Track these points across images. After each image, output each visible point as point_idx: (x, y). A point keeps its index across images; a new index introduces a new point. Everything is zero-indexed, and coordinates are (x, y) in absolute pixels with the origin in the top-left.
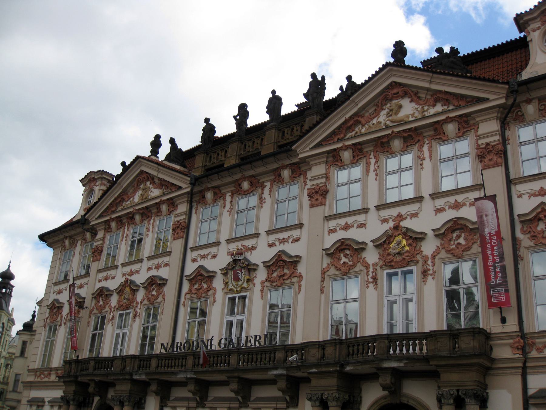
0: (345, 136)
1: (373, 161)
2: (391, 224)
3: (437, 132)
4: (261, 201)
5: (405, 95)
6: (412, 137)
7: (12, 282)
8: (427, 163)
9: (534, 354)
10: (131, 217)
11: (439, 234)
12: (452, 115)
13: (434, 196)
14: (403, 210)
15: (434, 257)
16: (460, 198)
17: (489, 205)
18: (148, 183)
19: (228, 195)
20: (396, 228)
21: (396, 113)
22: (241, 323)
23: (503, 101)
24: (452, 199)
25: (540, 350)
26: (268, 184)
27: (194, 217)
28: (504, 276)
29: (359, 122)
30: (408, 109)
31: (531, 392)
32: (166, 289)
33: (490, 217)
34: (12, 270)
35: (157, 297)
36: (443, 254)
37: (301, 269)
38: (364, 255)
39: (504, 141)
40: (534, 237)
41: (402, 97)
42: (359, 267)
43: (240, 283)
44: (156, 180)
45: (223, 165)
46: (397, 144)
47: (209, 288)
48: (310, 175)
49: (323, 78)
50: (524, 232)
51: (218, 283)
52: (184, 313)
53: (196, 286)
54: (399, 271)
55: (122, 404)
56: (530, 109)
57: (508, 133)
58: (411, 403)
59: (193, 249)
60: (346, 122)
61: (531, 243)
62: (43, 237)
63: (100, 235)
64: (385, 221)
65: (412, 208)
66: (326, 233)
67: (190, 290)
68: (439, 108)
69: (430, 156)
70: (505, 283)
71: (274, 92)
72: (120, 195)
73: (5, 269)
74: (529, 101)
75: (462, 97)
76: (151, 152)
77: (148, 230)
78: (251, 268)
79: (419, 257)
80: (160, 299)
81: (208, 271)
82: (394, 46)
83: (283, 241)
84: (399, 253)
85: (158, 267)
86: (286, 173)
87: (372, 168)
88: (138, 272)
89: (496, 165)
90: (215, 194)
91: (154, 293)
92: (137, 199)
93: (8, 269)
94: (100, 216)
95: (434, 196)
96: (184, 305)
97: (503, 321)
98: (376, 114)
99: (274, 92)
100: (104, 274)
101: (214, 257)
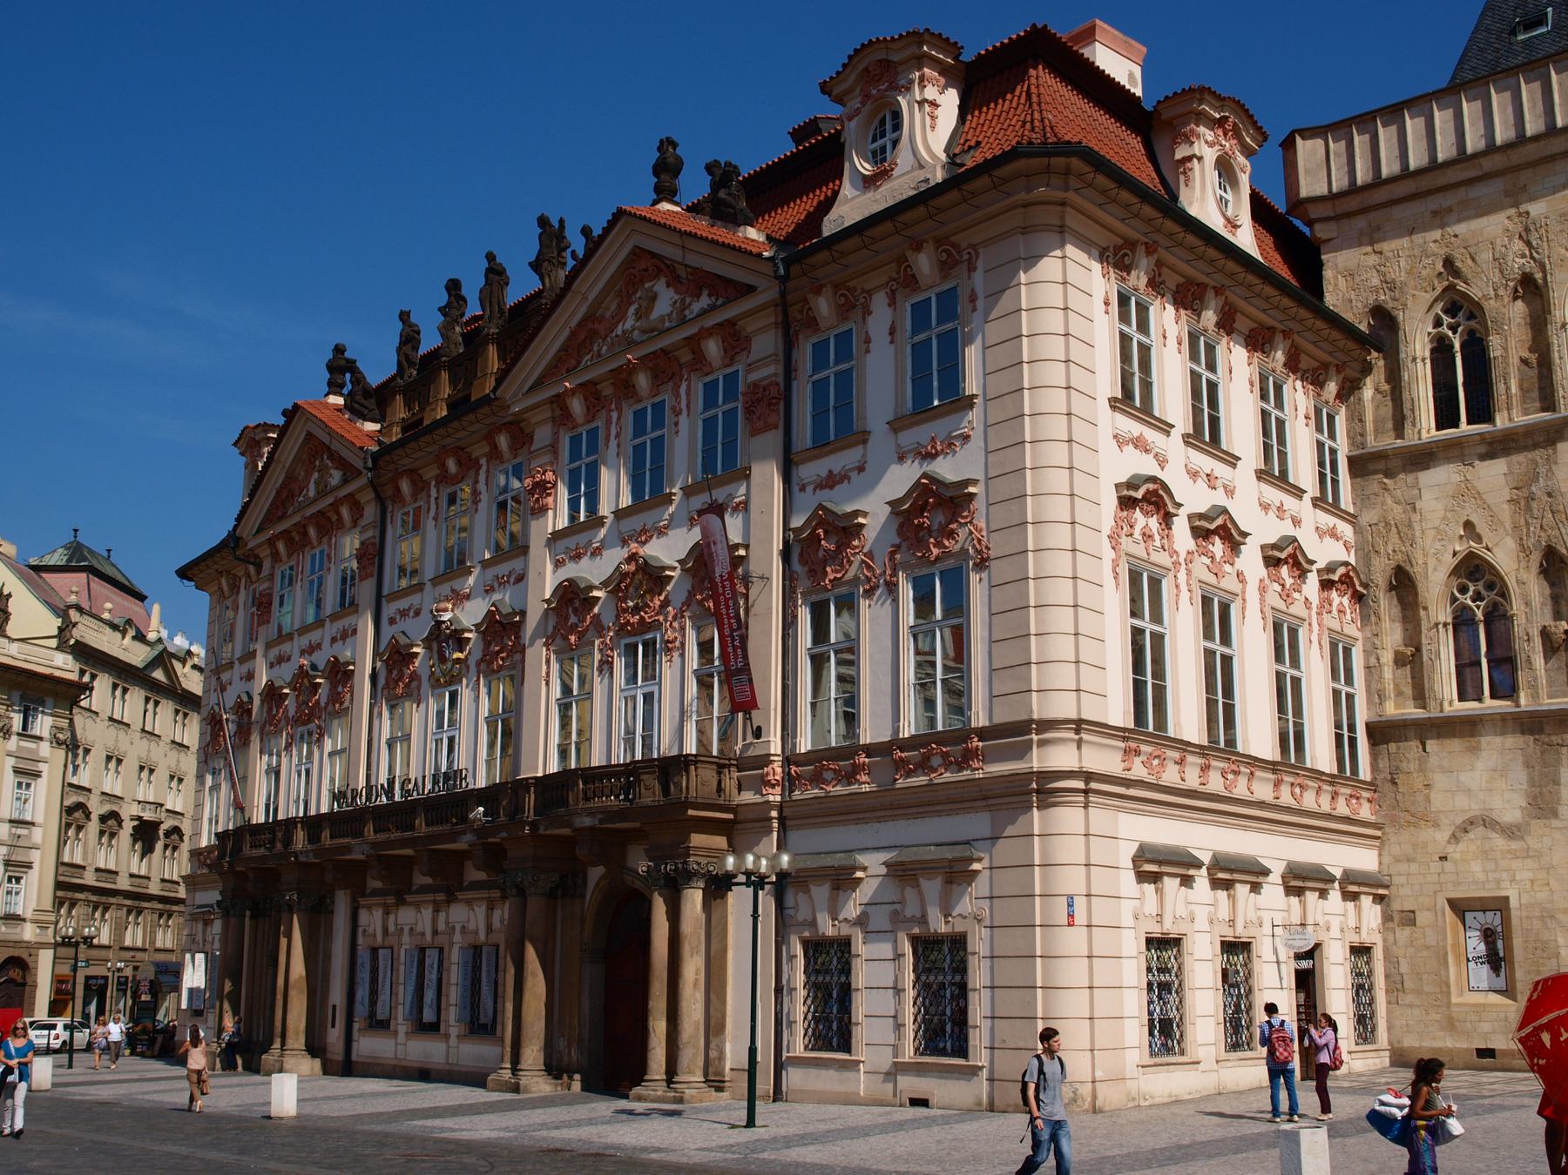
0: (579, 362)
1: (615, 415)
4: (475, 493)
12: (709, 322)
20: (632, 558)
21: (649, 309)
26: (483, 461)
30: (665, 300)
33: (719, 545)
39: (789, 371)
41: (656, 277)
43: (449, 665)
45: (421, 421)
49: (561, 221)
54: (639, 639)
56: (823, 306)
61: (809, 583)
62: (184, 573)
67: (387, 682)
68: (705, 301)
69: (688, 406)
71: (490, 257)
74: (818, 291)
75: (729, 282)
76: (330, 384)
82: (659, 149)
87: (613, 432)
90: (413, 483)
92: (312, 493)
94: (260, 530)
97: (758, 733)
98: (620, 316)
99: (490, 257)
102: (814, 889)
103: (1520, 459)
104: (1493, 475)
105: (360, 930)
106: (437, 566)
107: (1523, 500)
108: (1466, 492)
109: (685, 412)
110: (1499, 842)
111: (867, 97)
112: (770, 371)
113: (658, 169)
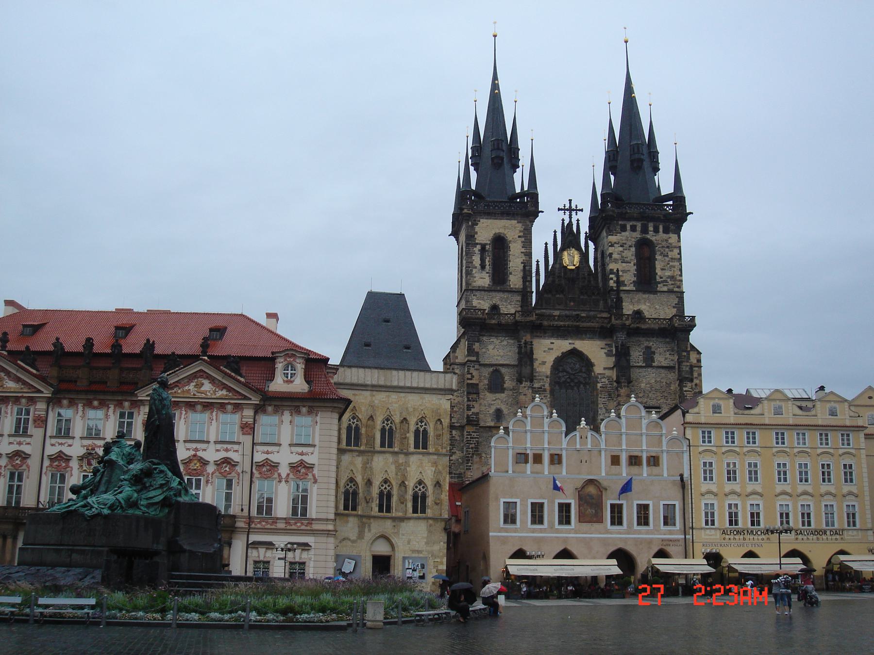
3: (222, 407)
4: (107, 416)
6: (208, 406)
8: (214, 422)
9: (253, 526)
13: (216, 442)
14: (199, 446)
15: (213, 474)
16: (229, 446)
20: (195, 456)
24: (225, 446)
26: (112, 407)
27: (50, 412)
29: (177, 386)
30: (207, 386)
32: (29, 461)
36: (217, 474)
39: (255, 420)
40: (260, 473)
44: (12, 376)
46: (199, 407)
47: (67, 466)
48: (142, 408)
51: (74, 464)
52: (46, 480)
53: (56, 463)
56: (270, 409)
59: (51, 437)
65: (204, 446)
75: (238, 392)
77: (7, 413)
80: (24, 467)
81: (66, 456)
85: (20, 443)
87: (183, 416)
89: (249, 434)
91: (18, 462)
95: (216, 442)
96: (46, 473)
97: (242, 510)
101: (70, 446)
103: (365, 458)
104: (359, 461)
106: (83, 433)
107: (365, 468)
108: (352, 463)
110: (349, 543)
111: (285, 360)
112: (251, 421)
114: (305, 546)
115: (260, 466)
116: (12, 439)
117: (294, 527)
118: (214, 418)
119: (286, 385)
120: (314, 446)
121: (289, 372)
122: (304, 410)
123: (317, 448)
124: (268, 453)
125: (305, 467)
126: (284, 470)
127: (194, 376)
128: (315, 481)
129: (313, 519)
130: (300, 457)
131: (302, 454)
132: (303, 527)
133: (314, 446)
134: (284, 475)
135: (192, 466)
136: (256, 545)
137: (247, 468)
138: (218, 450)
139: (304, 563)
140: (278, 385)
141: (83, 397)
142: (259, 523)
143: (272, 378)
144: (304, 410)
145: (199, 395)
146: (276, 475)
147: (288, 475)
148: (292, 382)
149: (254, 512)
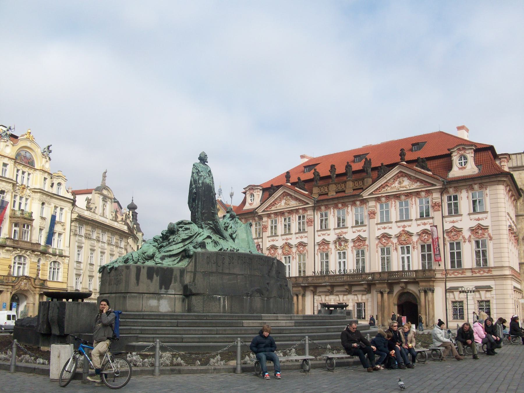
2: (402, 229)
3: (418, 194)
5: (406, 176)
6: (409, 195)
7: (136, 211)
8: (414, 205)
9: (449, 276)
10: (282, 213)
11: (419, 235)
15: (417, 242)
17: (434, 228)
18: (288, 197)
19: (332, 208)
22: (344, 262)
23: (441, 187)
25: (450, 275)
26: (350, 206)
28: (439, 252)
29: (387, 185)
31: (447, 288)
32: (307, 247)
34: (135, 203)
35: (303, 251)
36: (420, 241)
37: (367, 242)
38: (392, 239)
42: (390, 244)
45: (327, 194)
47: (328, 248)
50: (447, 235)
51: (332, 246)
52: (318, 258)
53: (322, 247)
55: (297, 296)
57: (443, 198)
58: (411, 292)
59: (318, 231)
60: (382, 185)
61: (449, 240)
63: (265, 219)
64: (399, 227)
66: (376, 229)
69: (415, 204)
70: (440, 254)
72: (273, 202)
73: (130, 202)
74: (451, 188)
78: (346, 241)
79: (411, 242)
80: (305, 251)
83: (359, 231)
84: (405, 240)
85: (301, 237)
86: (358, 203)
88: (291, 239)
89: (439, 210)
93: (132, 202)
96: (317, 254)
97: (439, 265)
99: (348, 163)
100: (272, 238)
101: (329, 235)
102: (455, 292)
105: (315, 300)
109: (414, 205)
113: (400, 155)
114: (488, 289)
115: (448, 232)
116: (297, 235)
117: (478, 275)
118: (414, 203)
119: (461, 171)
120: (486, 212)
121: (463, 161)
122: (476, 187)
123: (489, 214)
124: (453, 222)
125: (482, 229)
126: (466, 234)
127: (397, 176)
128: (491, 239)
129: (492, 268)
130: (477, 222)
131: (478, 220)
132: (485, 274)
133: (486, 212)
134: (467, 237)
135: (403, 238)
136: (452, 290)
137: (441, 235)
138: (418, 225)
139: (489, 301)
140: (456, 172)
141: (332, 202)
142: (453, 273)
143: (450, 167)
144: (476, 187)
145: (402, 189)
146: (461, 238)
147: (470, 236)
148: (465, 168)
149: (449, 267)
